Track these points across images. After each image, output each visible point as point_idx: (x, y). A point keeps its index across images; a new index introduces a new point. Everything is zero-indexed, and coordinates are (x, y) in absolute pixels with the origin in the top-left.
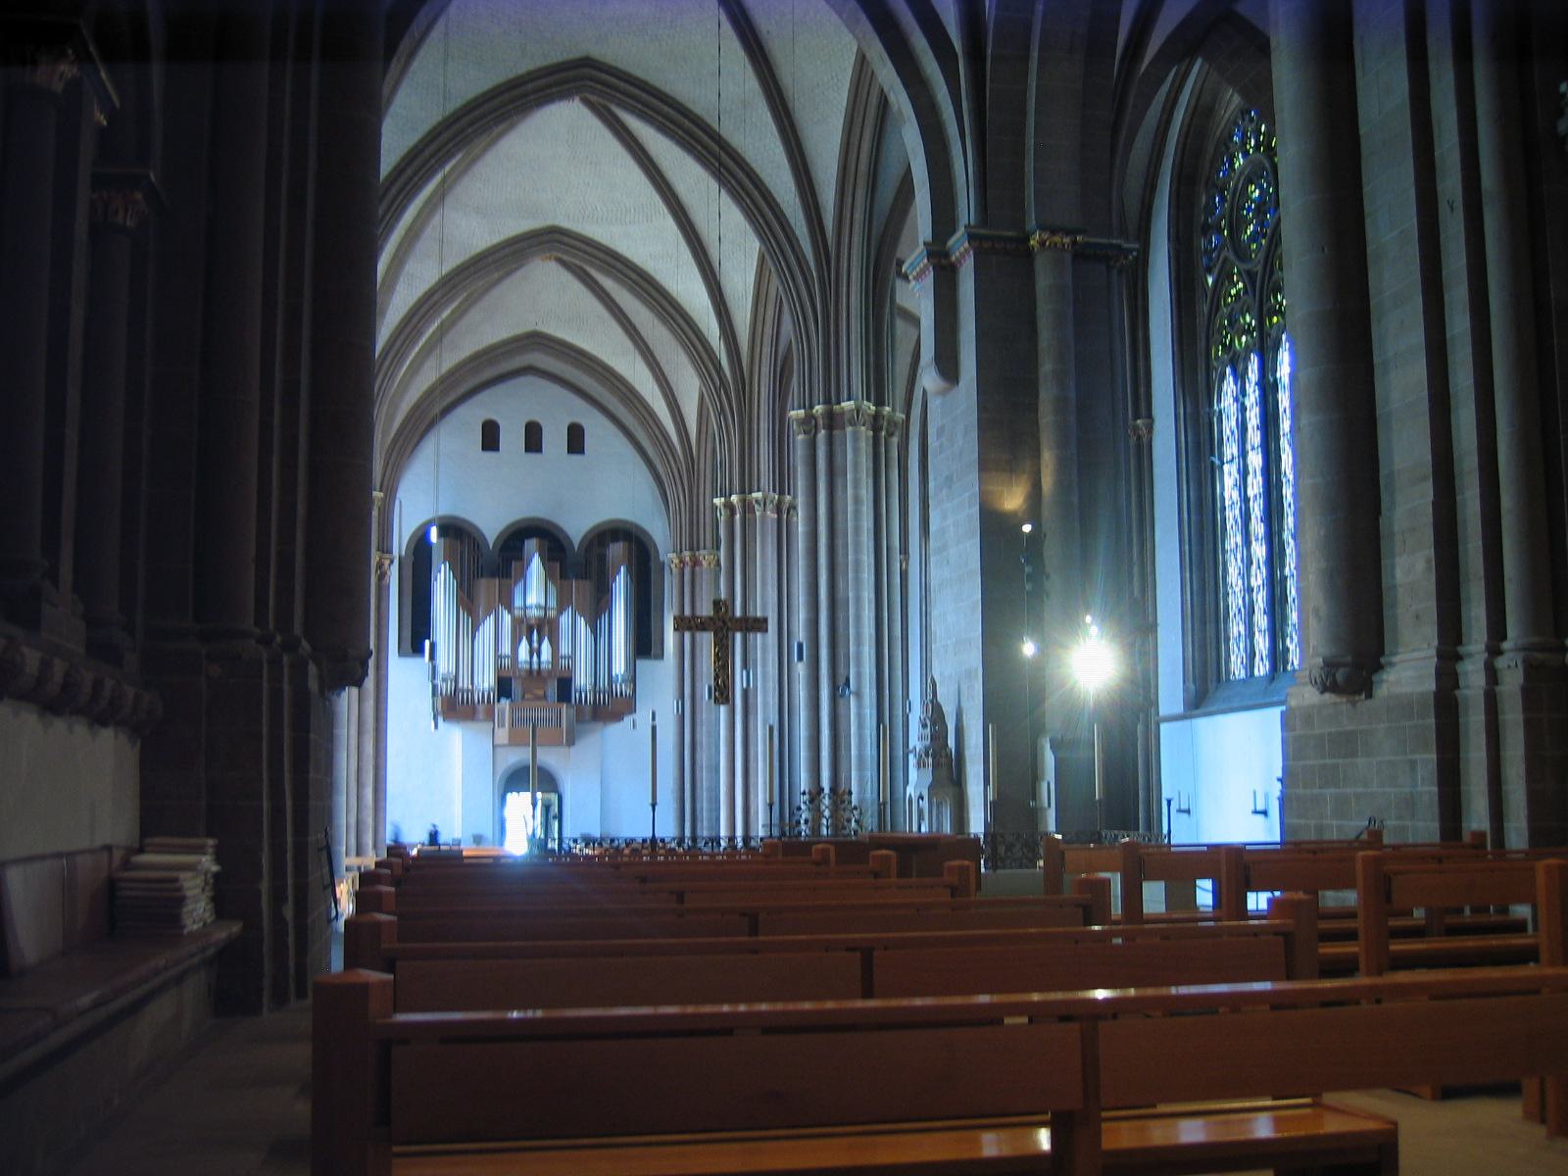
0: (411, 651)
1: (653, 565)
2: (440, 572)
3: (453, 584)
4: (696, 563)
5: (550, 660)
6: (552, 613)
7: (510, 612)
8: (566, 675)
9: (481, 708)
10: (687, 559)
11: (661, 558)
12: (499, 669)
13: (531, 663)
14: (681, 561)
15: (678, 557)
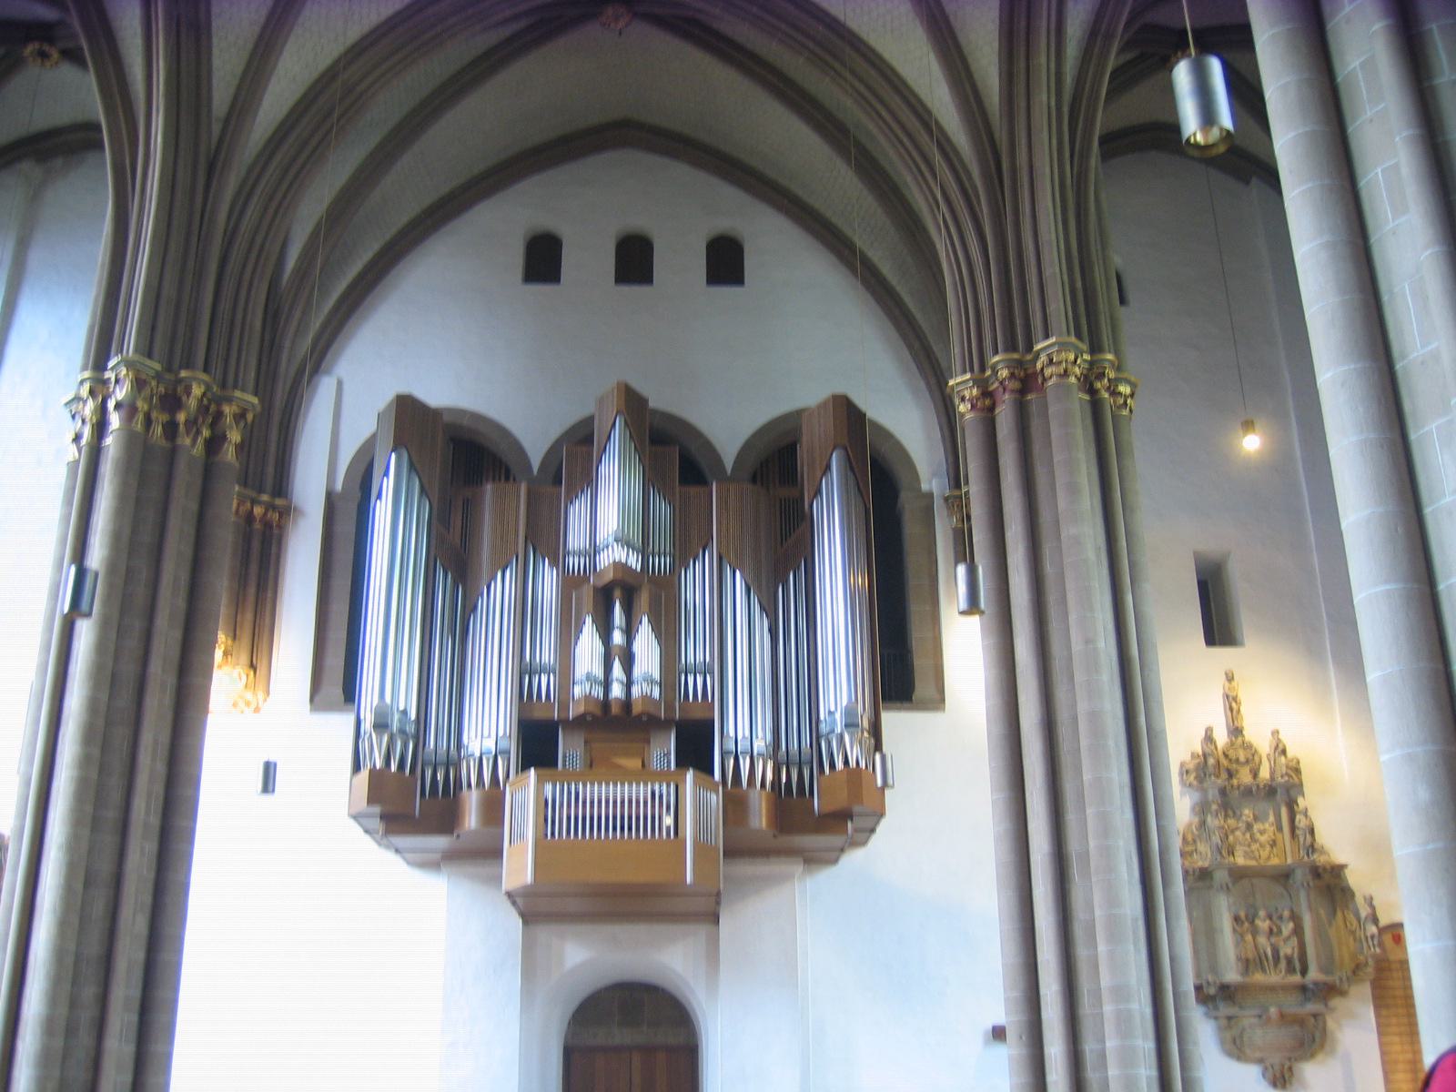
1: (905, 498)
2: (386, 474)
3: (420, 511)
4: (1027, 381)
5: (657, 676)
6: (661, 563)
7: (554, 563)
8: (698, 714)
9: (472, 802)
10: (1004, 373)
11: (925, 487)
12: (525, 699)
13: (607, 685)
14: (986, 393)
15: (977, 382)
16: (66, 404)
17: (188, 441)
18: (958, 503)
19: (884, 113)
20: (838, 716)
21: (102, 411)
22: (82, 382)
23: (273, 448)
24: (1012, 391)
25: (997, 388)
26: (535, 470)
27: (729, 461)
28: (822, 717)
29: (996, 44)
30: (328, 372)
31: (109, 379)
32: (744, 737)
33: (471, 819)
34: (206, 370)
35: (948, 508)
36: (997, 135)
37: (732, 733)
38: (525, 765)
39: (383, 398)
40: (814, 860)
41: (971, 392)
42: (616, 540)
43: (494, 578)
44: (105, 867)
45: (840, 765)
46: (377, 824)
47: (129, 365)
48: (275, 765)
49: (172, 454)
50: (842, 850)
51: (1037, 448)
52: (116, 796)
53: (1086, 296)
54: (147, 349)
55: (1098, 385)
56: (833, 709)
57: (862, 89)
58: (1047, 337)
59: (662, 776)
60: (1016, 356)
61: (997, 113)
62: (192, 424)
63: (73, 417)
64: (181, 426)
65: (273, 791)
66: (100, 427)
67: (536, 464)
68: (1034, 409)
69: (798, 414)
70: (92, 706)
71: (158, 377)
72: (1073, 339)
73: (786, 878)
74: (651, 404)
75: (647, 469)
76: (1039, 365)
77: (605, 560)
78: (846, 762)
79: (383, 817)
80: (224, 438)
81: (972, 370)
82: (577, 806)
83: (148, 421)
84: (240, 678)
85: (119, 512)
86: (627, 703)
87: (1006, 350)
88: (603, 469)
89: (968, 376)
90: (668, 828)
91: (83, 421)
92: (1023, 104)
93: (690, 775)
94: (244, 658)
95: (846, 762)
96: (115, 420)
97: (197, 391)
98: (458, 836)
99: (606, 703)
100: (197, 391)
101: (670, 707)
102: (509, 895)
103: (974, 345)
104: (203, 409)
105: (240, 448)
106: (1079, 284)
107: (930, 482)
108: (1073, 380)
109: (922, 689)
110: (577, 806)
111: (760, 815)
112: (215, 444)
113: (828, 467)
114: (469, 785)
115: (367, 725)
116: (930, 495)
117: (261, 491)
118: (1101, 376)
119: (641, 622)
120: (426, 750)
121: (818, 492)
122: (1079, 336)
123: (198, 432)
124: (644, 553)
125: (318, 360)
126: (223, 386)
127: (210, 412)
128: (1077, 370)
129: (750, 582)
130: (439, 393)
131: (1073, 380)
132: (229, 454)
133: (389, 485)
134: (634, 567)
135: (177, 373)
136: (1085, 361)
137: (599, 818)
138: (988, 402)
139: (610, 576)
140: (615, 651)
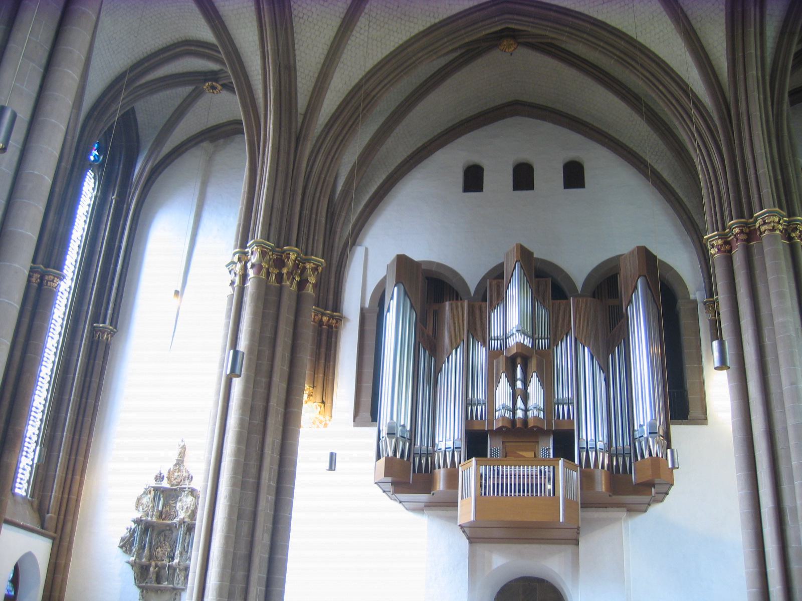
0: (371, 419)
1: (682, 307)
2: (392, 298)
3: (411, 316)
4: (750, 235)
5: (541, 406)
6: (543, 343)
7: (484, 345)
8: (566, 427)
9: (441, 475)
10: (737, 230)
11: (692, 297)
12: (469, 420)
13: (514, 411)
14: (727, 243)
15: (721, 236)
16: (227, 266)
17: (288, 283)
18: (712, 306)
19: (661, 87)
20: (645, 428)
21: (245, 268)
22: (234, 254)
23: (332, 286)
24: (742, 240)
25: (733, 238)
26: (472, 295)
27: (579, 283)
28: (636, 428)
29: (724, 45)
30: (360, 245)
31: (248, 252)
32: (591, 439)
33: (440, 485)
34: (297, 246)
35: (706, 309)
36: (727, 95)
37: (584, 437)
38: (469, 457)
39: (391, 257)
40: (634, 510)
41: (718, 242)
42: (517, 331)
43: (451, 353)
44: (248, 508)
45: (647, 456)
46: (389, 487)
47: (258, 244)
48: (336, 454)
49: (280, 290)
50: (649, 505)
51: (758, 272)
52: (253, 471)
53: (784, 184)
54: (267, 236)
55: (793, 235)
56: (642, 423)
57: (648, 75)
58: (762, 209)
59: (544, 462)
60: (743, 220)
61: (727, 84)
62: (290, 274)
63: (230, 272)
64: (285, 275)
65: (335, 470)
66: (244, 277)
67: (472, 290)
68: (755, 250)
69: (619, 257)
70: (241, 423)
71: (272, 250)
72: (777, 209)
73: (617, 520)
74: (535, 256)
75: (534, 292)
76: (757, 225)
77: (511, 342)
78: (650, 454)
79: (393, 483)
80: (307, 281)
81: (718, 230)
82: (498, 478)
83: (268, 274)
84: (317, 408)
85: (254, 321)
86: (525, 421)
87: (738, 218)
88: (510, 292)
89: (716, 233)
90: (549, 490)
91: (235, 274)
92: (742, 76)
93: (561, 462)
94: (319, 399)
95: (650, 454)
96: (251, 273)
97: (293, 257)
98: (433, 494)
99: (513, 421)
100: (293, 257)
101: (549, 423)
102: (461, 527)
103: (718, 214)
104: (296, 266)
105: (315, 286)
106: (780, 177)
107: (695, 294)
108: (778, 232)
109: (694, 412)
110: (498, 478)
111: (601, 485)
112: (302, 284)
113: (636, 288)
114: (439, 467)
115: (384, 433)
116: (695, 301)
117: (326, 309)
118: (795, 229)
119: (532, 377)
120: (415, 446)
121: (631, 301)
122: (781, 207)
123: (294, 278)
124: (533, 338)
125: (355, 238)
126: (306, 254)
127: (300, 267)
128: (780, 227)
129: (592, 353)
130: (418, 254)
131: (778, 232)
132: (310, 289)
133: (393, 304)
134: (528, 345)
135: (282, 248)
136: (785, 221)
137: (511, 485)
138: (727, 247)
139: (514, 351)
140: (518, 392)
